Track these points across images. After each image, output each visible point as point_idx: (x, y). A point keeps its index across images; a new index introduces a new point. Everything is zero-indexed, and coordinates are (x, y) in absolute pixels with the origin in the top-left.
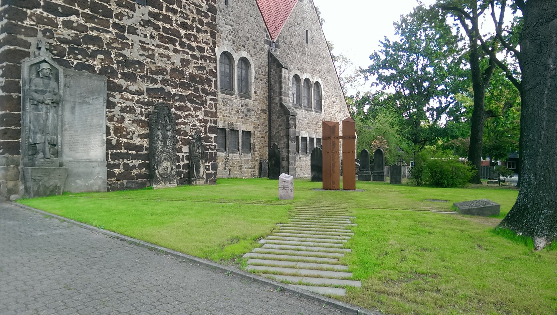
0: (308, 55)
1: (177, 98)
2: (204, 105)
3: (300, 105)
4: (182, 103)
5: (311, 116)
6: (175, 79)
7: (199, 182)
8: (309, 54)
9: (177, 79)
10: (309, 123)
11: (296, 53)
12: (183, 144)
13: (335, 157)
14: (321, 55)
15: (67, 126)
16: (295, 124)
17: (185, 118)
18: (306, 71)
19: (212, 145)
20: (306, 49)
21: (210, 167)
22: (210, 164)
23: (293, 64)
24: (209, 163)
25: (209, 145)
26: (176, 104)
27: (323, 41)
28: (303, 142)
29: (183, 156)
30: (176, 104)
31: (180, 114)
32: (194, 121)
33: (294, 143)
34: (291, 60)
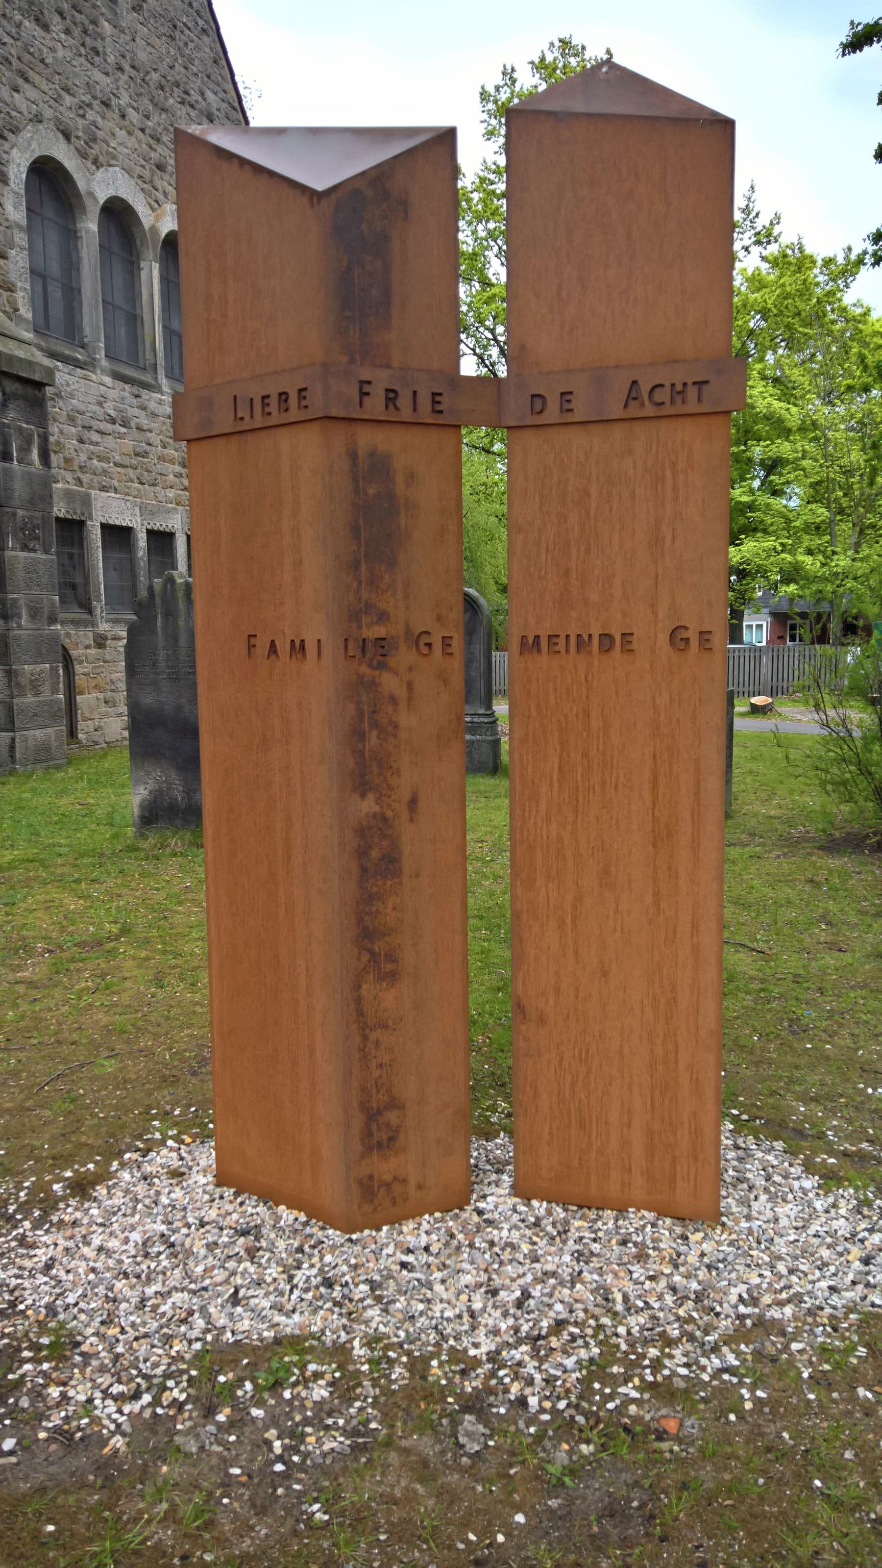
0: (120, 69)
3: (83, 346)
5: (154, 415)
8: (127, 67)
10: (145, 455)
11: (46, 27)
13: (405, 719)
14: (195, 96)
16: (44, 439)
18: (114, 157)
20: (106, 24)
23: (30, 92)
27: (201, 22)
28: (116, 555)
33: (40, 555)
34: (14, 61)
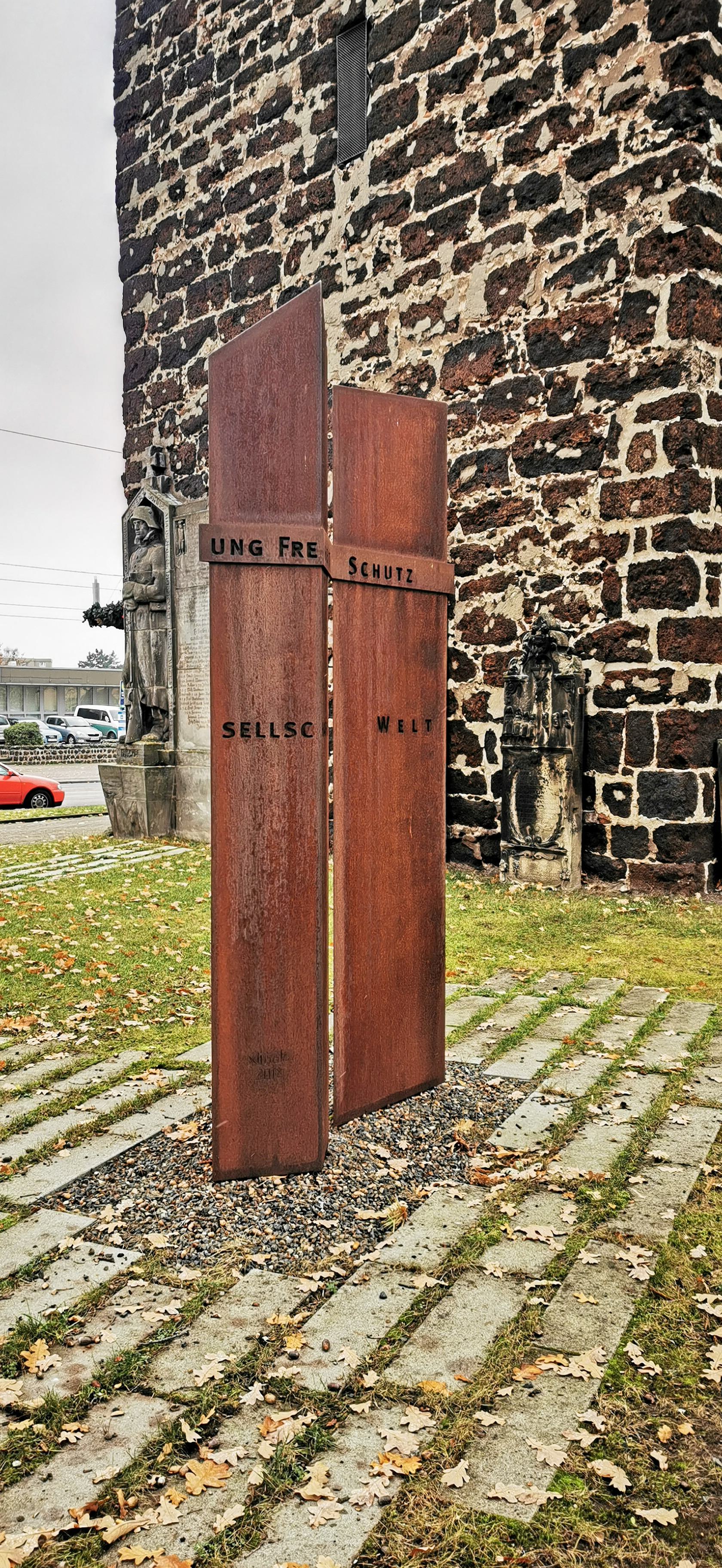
1: (468, 473)
2: (605, 461)
4: (492, 490)
6: (467, 390)
7: (533, 867)
9: (471, 388)
12: (491, 680)
15: (182, 659)
17: (501, 557)
19: (644, 675)
21: (635, 795)
22: (633, 781)
24: (626, 772)
25: (626, 676)
26: (465, 504)
29: (490, 734)
30: (469, 502)
31: (486, 542)
32: (545, 561)
